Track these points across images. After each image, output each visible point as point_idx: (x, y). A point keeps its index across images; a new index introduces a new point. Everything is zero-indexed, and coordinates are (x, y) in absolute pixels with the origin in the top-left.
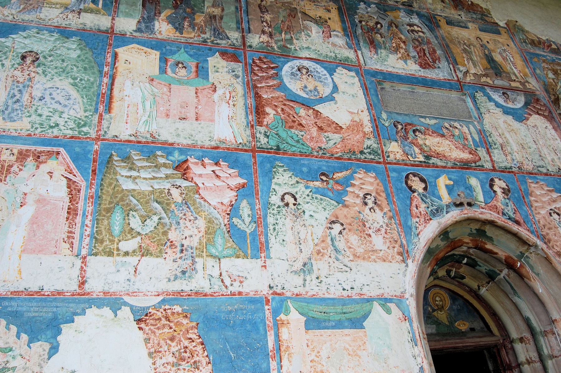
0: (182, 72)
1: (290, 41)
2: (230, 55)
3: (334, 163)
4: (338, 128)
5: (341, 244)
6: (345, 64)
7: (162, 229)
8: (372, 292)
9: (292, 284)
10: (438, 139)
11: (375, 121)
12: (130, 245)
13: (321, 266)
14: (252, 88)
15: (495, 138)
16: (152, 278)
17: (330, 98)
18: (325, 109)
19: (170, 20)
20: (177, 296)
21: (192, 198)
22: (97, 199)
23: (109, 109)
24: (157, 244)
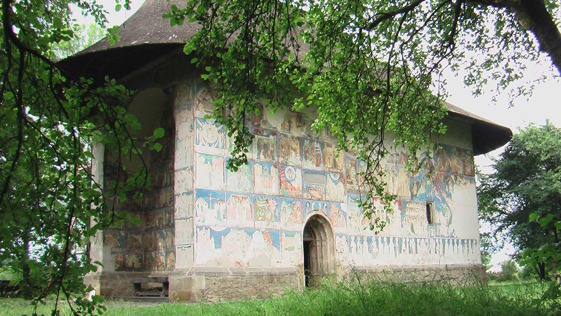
2: (276, 167)
3: (293, 199)
12: (260, 218)
15: (328, 191)
16: (263, 225)
19: (264, 154)
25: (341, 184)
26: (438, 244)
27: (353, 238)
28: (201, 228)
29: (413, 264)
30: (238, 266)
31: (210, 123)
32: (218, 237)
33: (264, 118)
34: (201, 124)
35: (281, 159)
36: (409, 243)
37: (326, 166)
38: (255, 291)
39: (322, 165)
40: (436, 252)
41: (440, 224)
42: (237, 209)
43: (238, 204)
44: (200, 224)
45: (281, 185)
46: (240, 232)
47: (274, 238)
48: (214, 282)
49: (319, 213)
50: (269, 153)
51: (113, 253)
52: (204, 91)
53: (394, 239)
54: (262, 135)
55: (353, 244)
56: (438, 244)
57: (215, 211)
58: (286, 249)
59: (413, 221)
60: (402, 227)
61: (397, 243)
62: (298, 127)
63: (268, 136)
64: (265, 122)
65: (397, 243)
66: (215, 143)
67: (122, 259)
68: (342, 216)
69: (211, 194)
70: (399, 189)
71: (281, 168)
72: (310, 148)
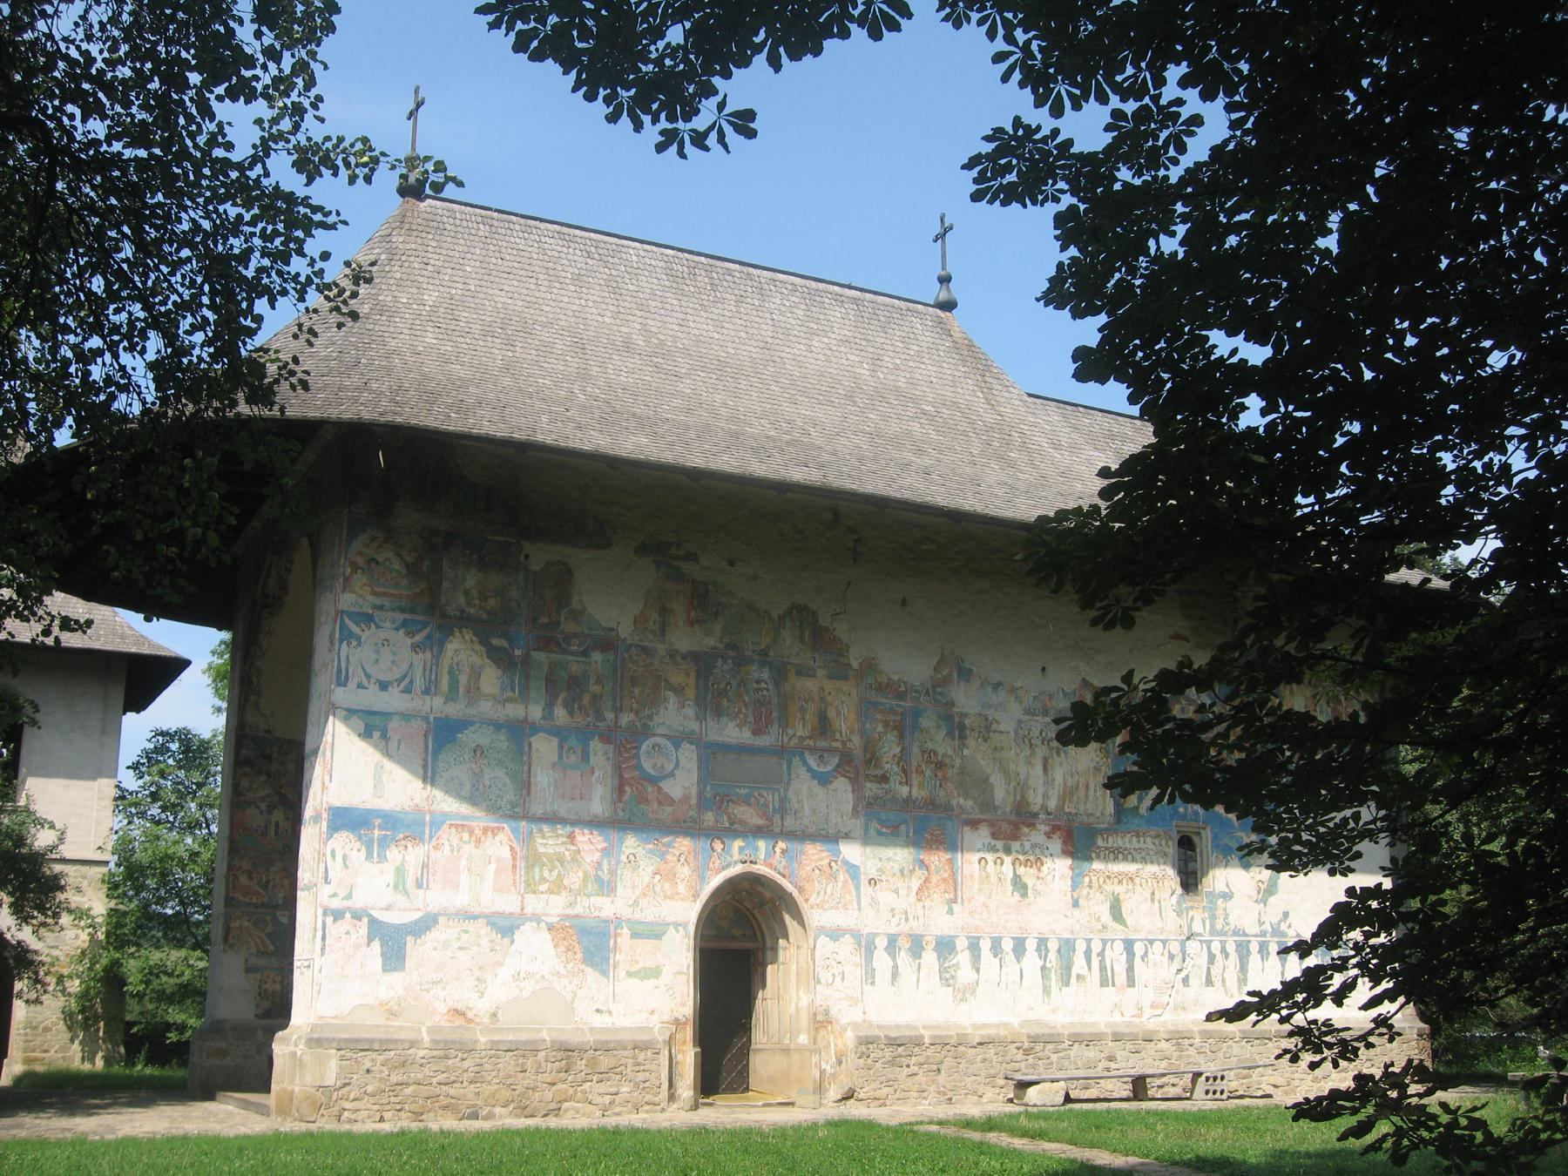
0: (573, 757)
1: (650, 717)
2: (606, 739)
4: (671, 801)
5: (658, 889)
6: (690, 738)
7: (560, 878)
8: (672, 919)
9: (627, 913)
10: (745, 808)
11: (700, 794)
12: (544, 887)
13: (643, 902)
14: (618, 769)
16: (554, 906)
17: (672, 775)
18: (666, 786)
19: (566, 705)
20: (568, 916)
21: (576, 858)
22: (526, 859)
23: (529, 793)
24: (557, 887)
25: (842, 785)
26: (1219, 957)
27: (881, 943)
28: (338, 915)
29: (1117, 1018)
30: (459, 1021)
31: (388, 624)
32: (393, 943)
33: (575, 604)
34: (355, 629)
35: (625, 719)
36: (1101, 954)
37: (791, 732)
38: (506, 1094)
39: (775, 728)
40: (1209, 982)
41: (1227, 896)
42: (463, 862)
43: (468, 848)
44: (336, 904)
45: (620, 791)
46: (470, 926)
47: (592, 944)
48: (368, 1065)
49: (760, 869)
50: (586, 700)
51: (248, 970)
52: (373, 539)
53: (1042, 943)
54: (565, 652)
55: (882, 960)
56: (1219, 957)
57: (389, 869)
58: (630, 974)
59: (1118, 889)
60: (1076, 904)
61: (1052, 955)
62: (692, 624)
63: (585, 653)
64: (576, 616)
65: (1052, 955)
66: (400, 681)
67: (278, 987)
68: (841, 877)
69: (377, 822)
70: (1068, 793)
71: (625, 744)
72: (734, 683)
